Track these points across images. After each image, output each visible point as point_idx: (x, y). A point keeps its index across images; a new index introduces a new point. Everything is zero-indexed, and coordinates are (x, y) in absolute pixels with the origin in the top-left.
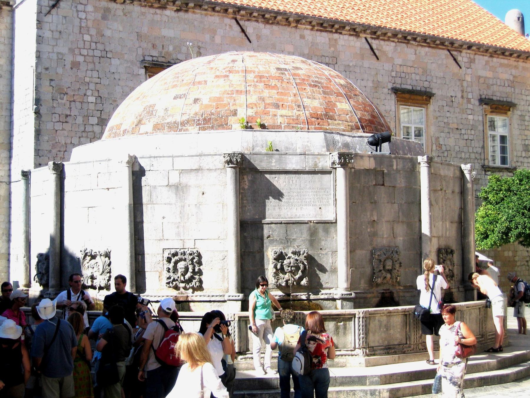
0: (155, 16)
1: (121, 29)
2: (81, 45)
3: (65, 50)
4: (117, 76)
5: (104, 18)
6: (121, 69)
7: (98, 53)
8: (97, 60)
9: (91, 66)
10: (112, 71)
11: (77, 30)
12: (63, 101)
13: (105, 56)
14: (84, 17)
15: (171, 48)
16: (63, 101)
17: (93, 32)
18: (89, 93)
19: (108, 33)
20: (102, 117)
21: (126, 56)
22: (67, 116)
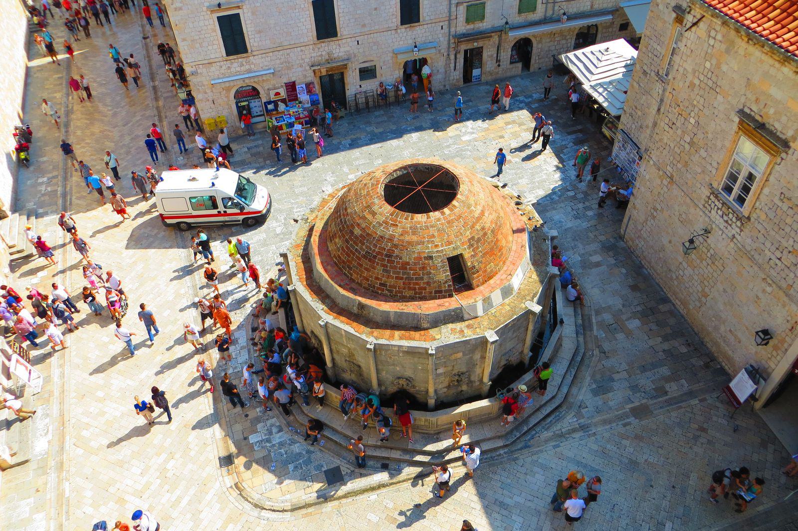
0: (772, 68)
1: (736, 68)
2: (701, 70)
3: (690, 69)
4: (716, 113)
5: (728, 51)
6: (721, 108)
7: (710, 83)
8: (707, 89)
9: (701, 92)
10: (715, 105)
11: (703, 55)
12: (675, 111)
13: (714, 89)
14: (712, 44)
15: (772, 111)
16: (675, 111)
17: (714, 62)
18: (692, 114)
19: (724, 68)
20: (695, 140)
21: (730, 98)
22: (673, 123)
